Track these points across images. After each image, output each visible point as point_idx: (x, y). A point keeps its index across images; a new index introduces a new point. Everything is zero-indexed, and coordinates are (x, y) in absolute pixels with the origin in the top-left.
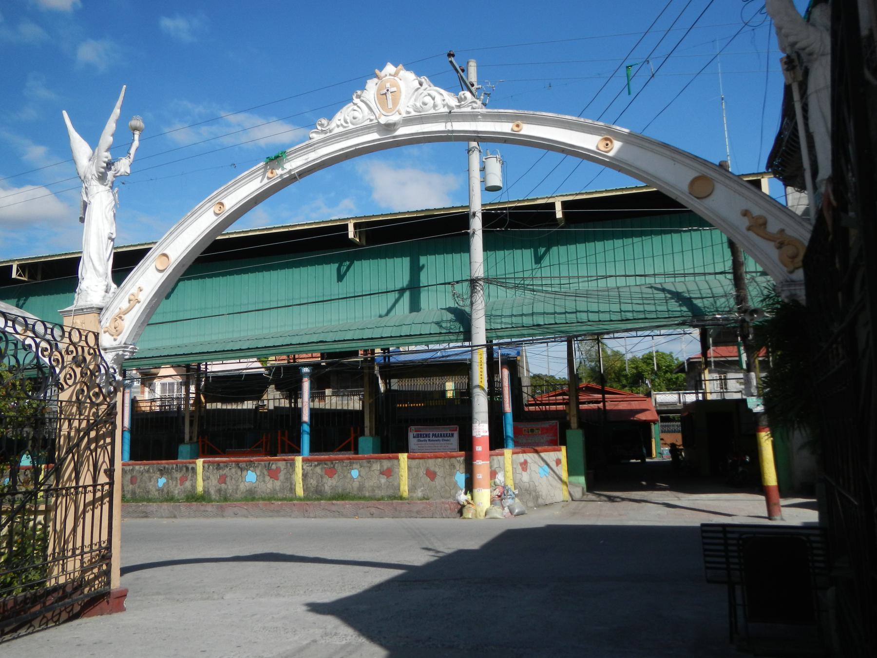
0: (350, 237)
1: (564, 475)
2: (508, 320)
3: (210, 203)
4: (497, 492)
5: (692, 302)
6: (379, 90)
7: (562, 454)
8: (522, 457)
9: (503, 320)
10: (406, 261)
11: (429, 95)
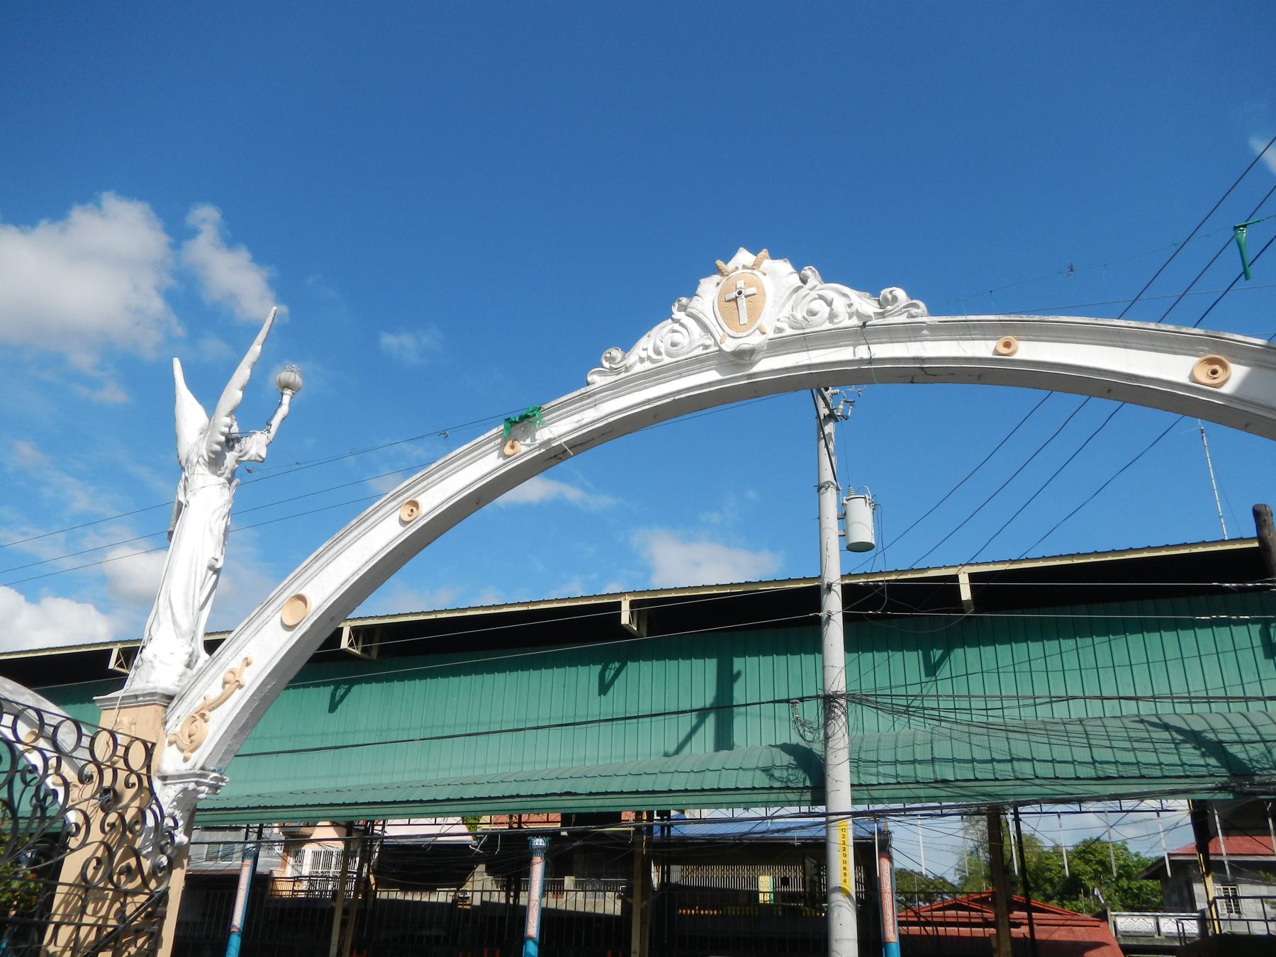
0: (623, 622)
2: (889, 770)
3: (394, 503)
5: (1224, 750)
9: (881, 769)
10: (712, 664)
11: (821, 297)
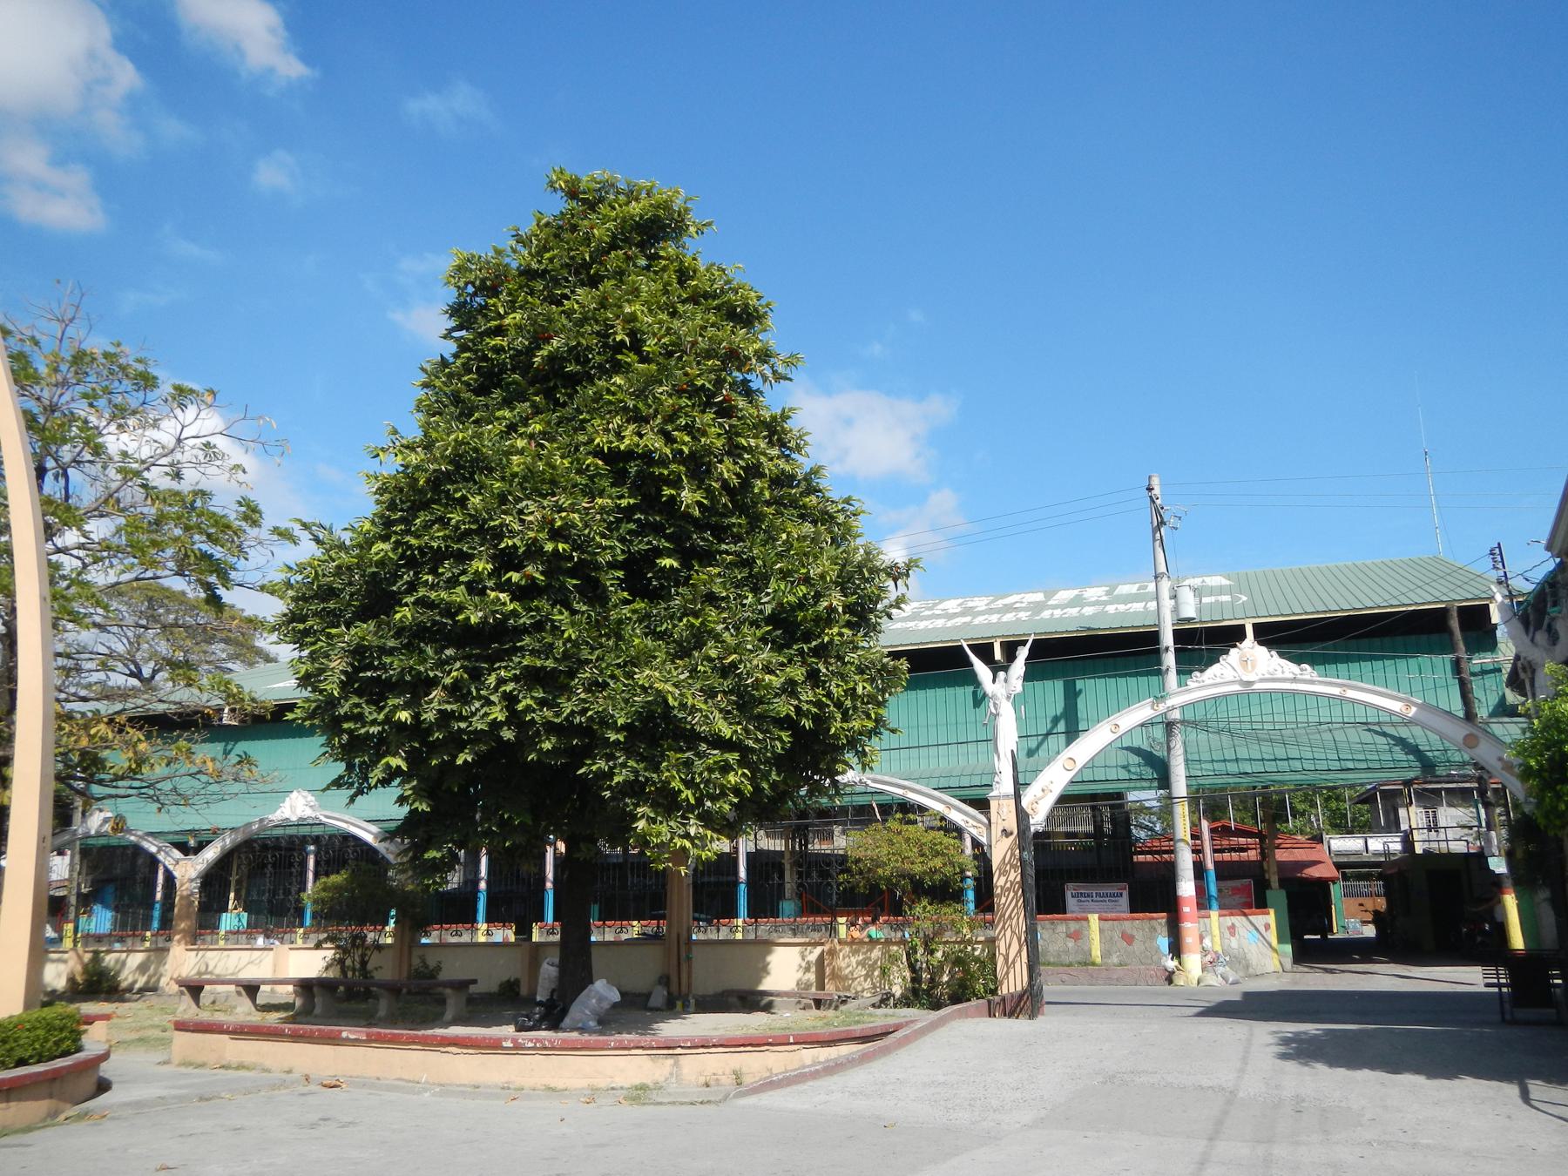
1: (1274, 942)
2: (1209, 766)
4: (1209, 958)
6: (1240, 658)
7: (1270, 918)
8: (1229, 920)
10: (1059, 685)
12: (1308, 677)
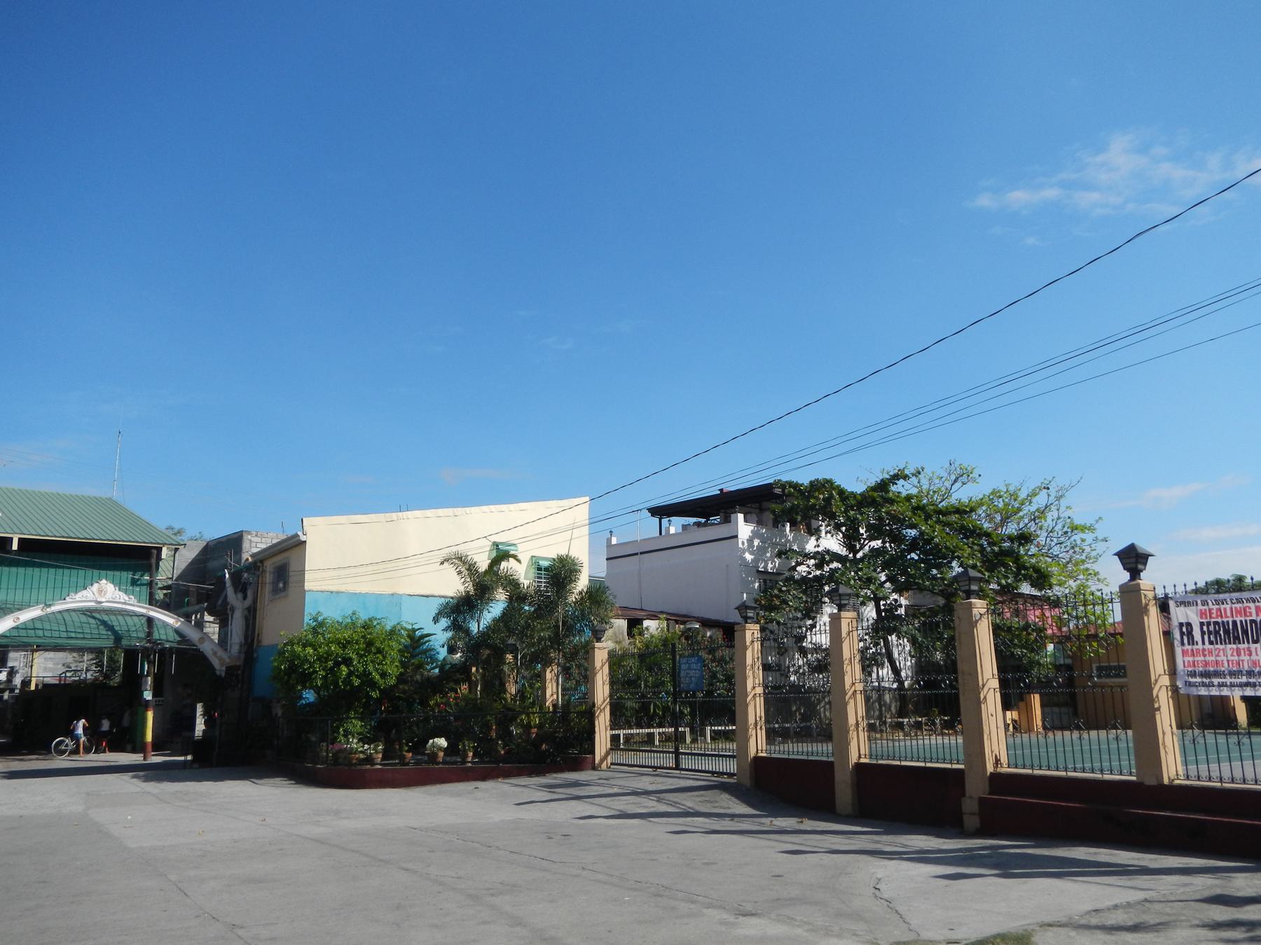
5: (114, 628)
12: (132, 603)
